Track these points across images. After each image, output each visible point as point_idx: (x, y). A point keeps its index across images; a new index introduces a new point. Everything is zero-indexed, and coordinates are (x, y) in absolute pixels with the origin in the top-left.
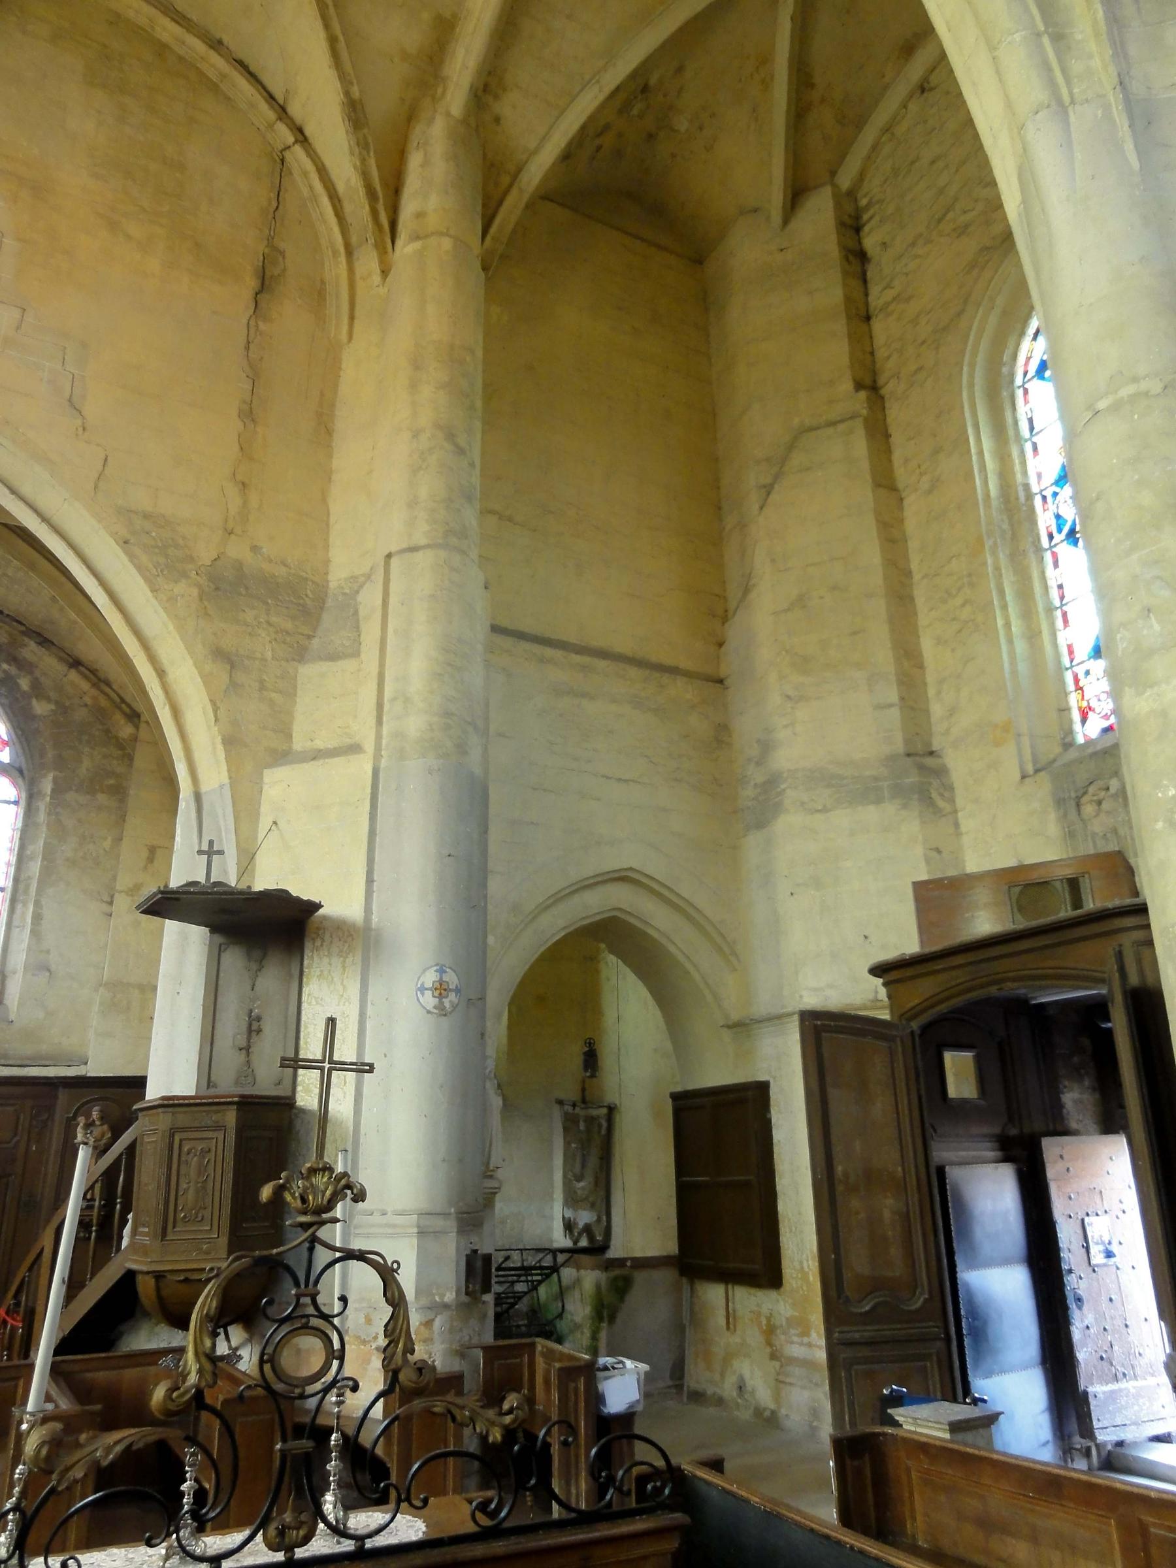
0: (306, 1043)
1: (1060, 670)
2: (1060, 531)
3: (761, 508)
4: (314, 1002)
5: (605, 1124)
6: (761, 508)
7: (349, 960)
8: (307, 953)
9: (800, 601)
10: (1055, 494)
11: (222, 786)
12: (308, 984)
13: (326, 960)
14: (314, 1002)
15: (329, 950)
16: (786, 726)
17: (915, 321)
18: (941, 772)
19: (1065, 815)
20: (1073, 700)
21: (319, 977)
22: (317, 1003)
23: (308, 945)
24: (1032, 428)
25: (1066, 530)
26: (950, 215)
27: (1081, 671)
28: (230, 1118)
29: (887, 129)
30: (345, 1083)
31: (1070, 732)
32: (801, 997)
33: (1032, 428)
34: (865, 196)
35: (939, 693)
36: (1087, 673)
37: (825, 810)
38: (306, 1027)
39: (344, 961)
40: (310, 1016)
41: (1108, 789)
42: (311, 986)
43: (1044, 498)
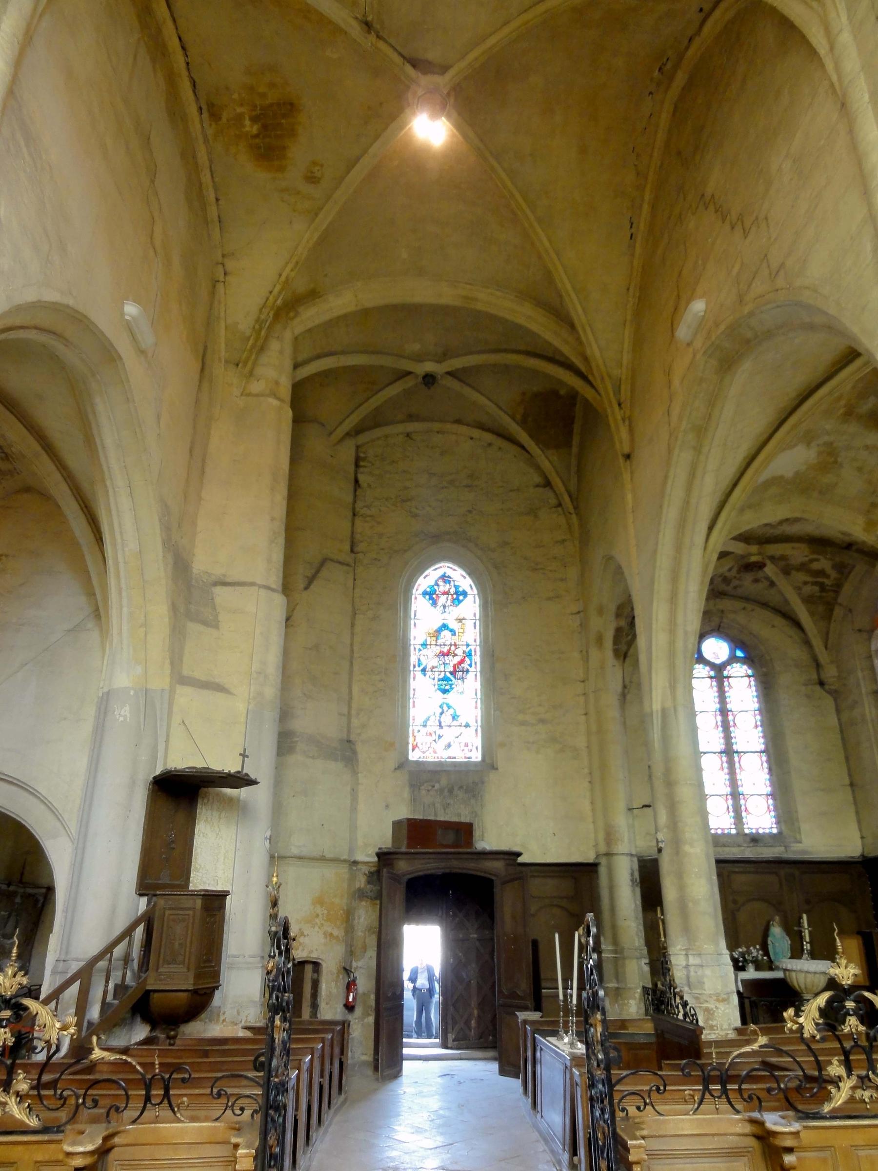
0: (196, 858)
1: (409, 726)
2: (419, 666)
3: (306, 588)
4: (201, 835)
5: (41, 899)
6: (306, 588)
7: (223, 814)
8: (199, 806)
9: (316, 647)
10: (420, 650)
11: (163, 690)
12: (198, 825)
13: (209, 812)
14: (201, 835)
15: (211, 807)
16: (302, 709)
17: (381, 535)
18: (354, 752)
19: (413, 791)
20: (411, 739)
21: (205, 821)
22: (204, 836)
23: (200, 801)
24: (415, 616)
25: (422, 667)
26: (408, 503)
27: (416, 729)
28: (199, 902)
29: (387, 436)
30: (217, 885)
31: (407, 754)
32: (291, 849)
33: (415, 616)
34: (364, 453)
35: (358, 714)
36: (419, 731)
37: (313, 758)
38: (196, 849)
39: (220, 815)
40: (199, 843)
41: (434, 787)
42: (200, 825)
43: (415, 649)
